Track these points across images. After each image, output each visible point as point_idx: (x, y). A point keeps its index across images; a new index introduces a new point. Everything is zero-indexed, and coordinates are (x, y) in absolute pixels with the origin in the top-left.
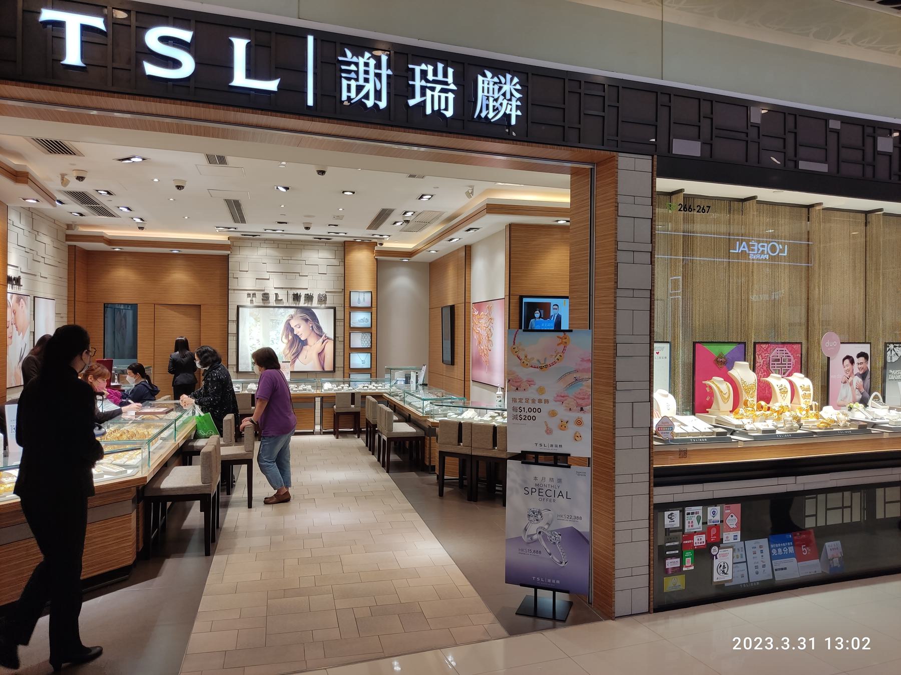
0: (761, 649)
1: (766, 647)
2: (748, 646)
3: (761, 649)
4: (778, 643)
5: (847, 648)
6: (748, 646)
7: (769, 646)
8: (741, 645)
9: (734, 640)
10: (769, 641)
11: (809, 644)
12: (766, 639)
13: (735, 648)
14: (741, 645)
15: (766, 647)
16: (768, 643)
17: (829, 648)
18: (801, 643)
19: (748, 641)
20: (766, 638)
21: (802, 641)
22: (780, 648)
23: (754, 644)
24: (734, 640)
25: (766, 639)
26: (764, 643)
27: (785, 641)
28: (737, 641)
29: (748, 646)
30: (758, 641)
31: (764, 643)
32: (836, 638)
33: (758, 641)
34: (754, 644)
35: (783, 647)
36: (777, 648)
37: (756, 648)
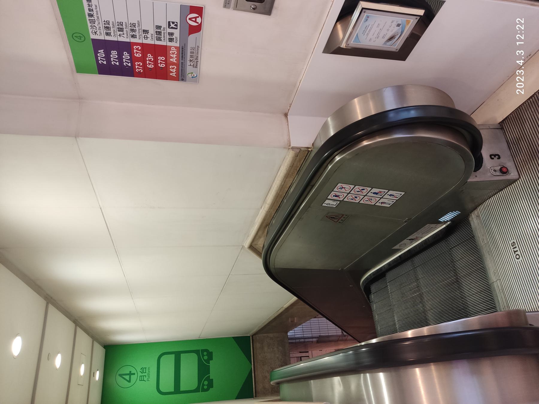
0: (523, 77)
1: (522, 74)
2: (522, 85)
3: (523, 77)
6: (521, 85)
7: (522, 72)
8: (521, 89)
9: (518, 93)
12: (518, 74)
13: (523, 93)
14: (521, 89)
15: (522, 74)
16: (520, 73)
17: (523, 43)
18: (520, 73)
19: (519, 85)
20: (517, 94)
23: (520, 81)
24: (518, 93)
25: (518, 74)
26: (520, 75)
27: (518, 53)
28: (518, 92)
29: (522, 85)
30: (518, 79)
32: (517, 75)
33: (518, 79)
34: (520, 81)
35: (522, 55)
37: (523, 80)
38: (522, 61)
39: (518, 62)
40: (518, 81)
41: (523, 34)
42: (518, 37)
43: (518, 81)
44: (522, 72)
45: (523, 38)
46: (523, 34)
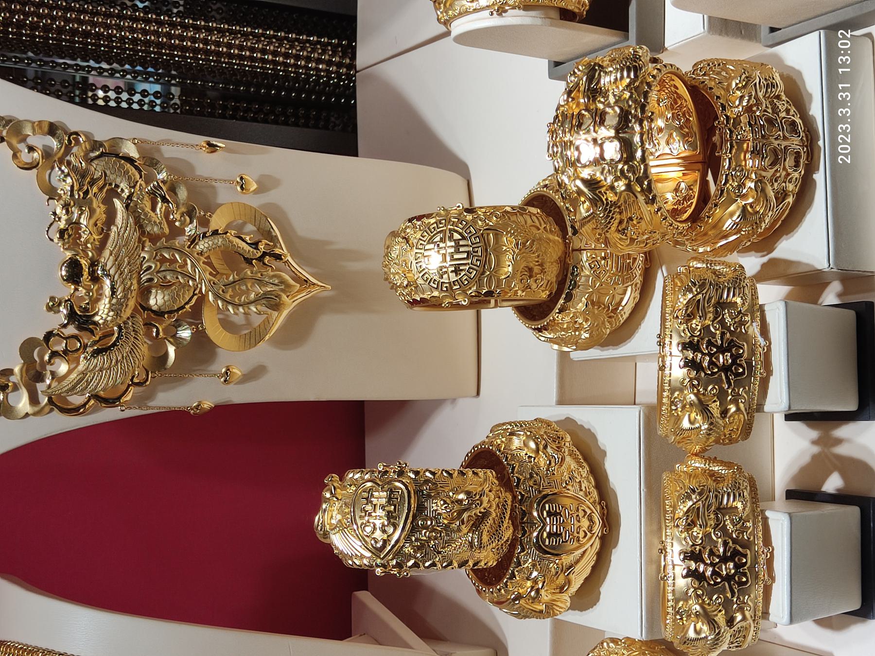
0: (849, 135)
1: (848, 131)
2: (847, 149)
3: (849, 135)
6: (846, 149)
7: (847, 128)
8: (846, 155)
9: (841, 162)
10: (841, 128)
12: (840, 131)
13: (849, 162)
14: (846, 155)
15: (848, 131)
16: (844, 129)
17: (849, 70)
21: (841, 96)
22: (849, 117)
23: (845, 142)
24: (841, 162)
25: (840, 131)
26: (844, 133)
27: (841, 112)
28: (841, 159)
29: (847, 149)
30: (841, 139)
31: (844, 133)
33: (841, 139)
34: (845, 142)
37: (849, 141)
40: (841, 141)
43: (841, 141)
44: (847, 128)
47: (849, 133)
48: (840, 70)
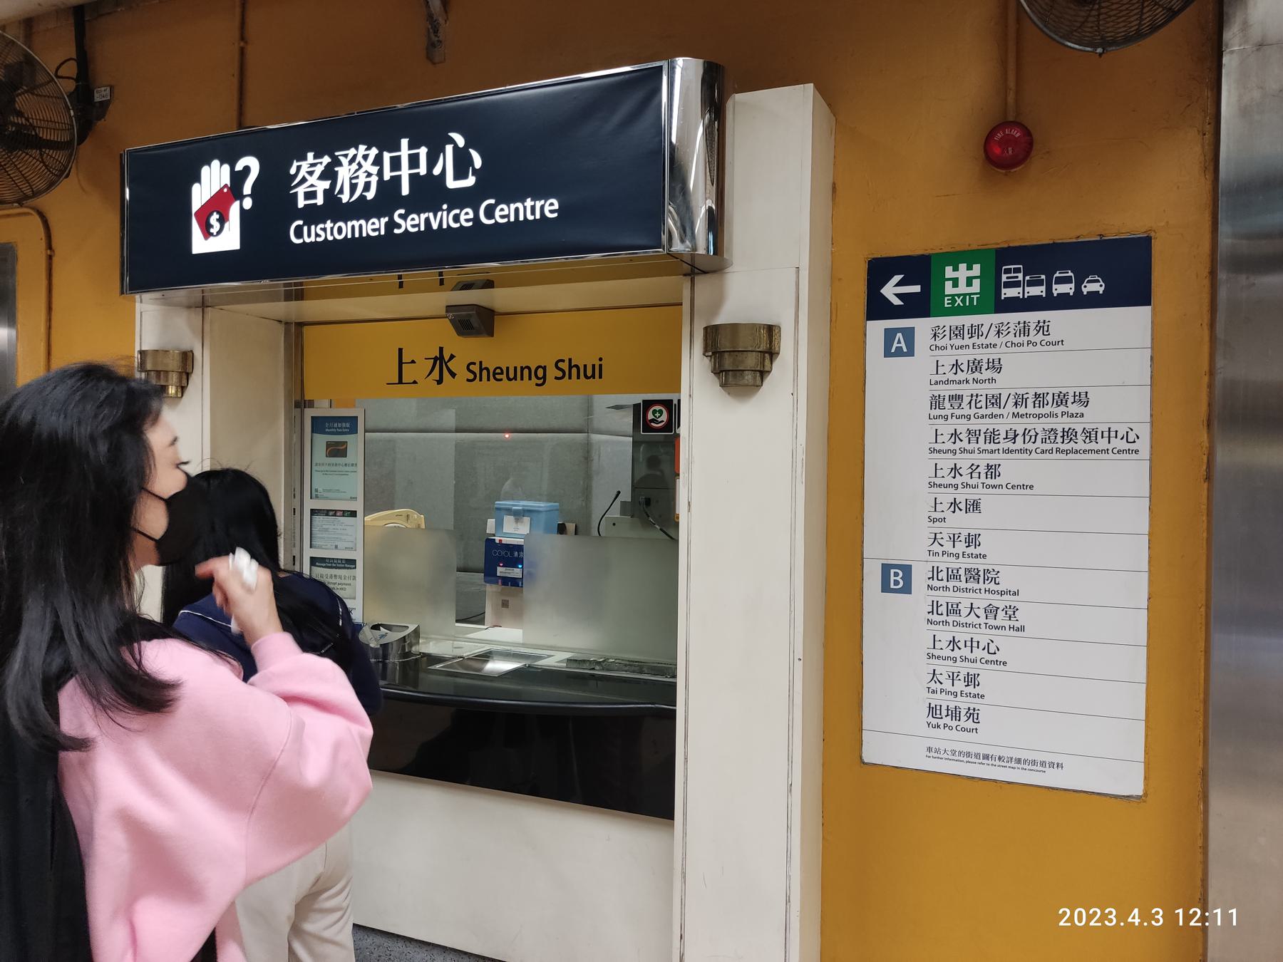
0: (1100, 924)
1: (1107, 923)
2: (1080, 921)
3: (1100, 924)
4: (1170, 917)
5: (1122, 924)
6: (1080, 920)
7: (1111, 921)
8: (1071, 919)
9: (1060, 912)
11: (1227, 917)
12: (1107, 911)
13: (1061, 924)
14: (1071, 919)
15: (1107, 923)
16: (1109, 917)
17: (1181, 924)
19: (1080, 913)
22: (1150, 924)
23: (1090, 918)
24: (1060, 912)
25: (1107, 911)
26: (1104, 917)
27: (1157, 913)
28: (1065, 913)
29: (1080, 921)
30: (1095, 913)
31: (1104, 917)
33: (1095, 913)
34: (1090, 918)
35: (1153, 922)
36: (1122, 924)
37: (1092, 924)
38: (1137, 921)
39: (1136, 911)
40: (1091, 912)
41: (1203, 924)
42: (1195, 913)
43: (1091, 912)
44: (1111, 921)
45: (1192, 924)
46: (1203, 924)
47: (1104, 925)
48: (1218, 911)
